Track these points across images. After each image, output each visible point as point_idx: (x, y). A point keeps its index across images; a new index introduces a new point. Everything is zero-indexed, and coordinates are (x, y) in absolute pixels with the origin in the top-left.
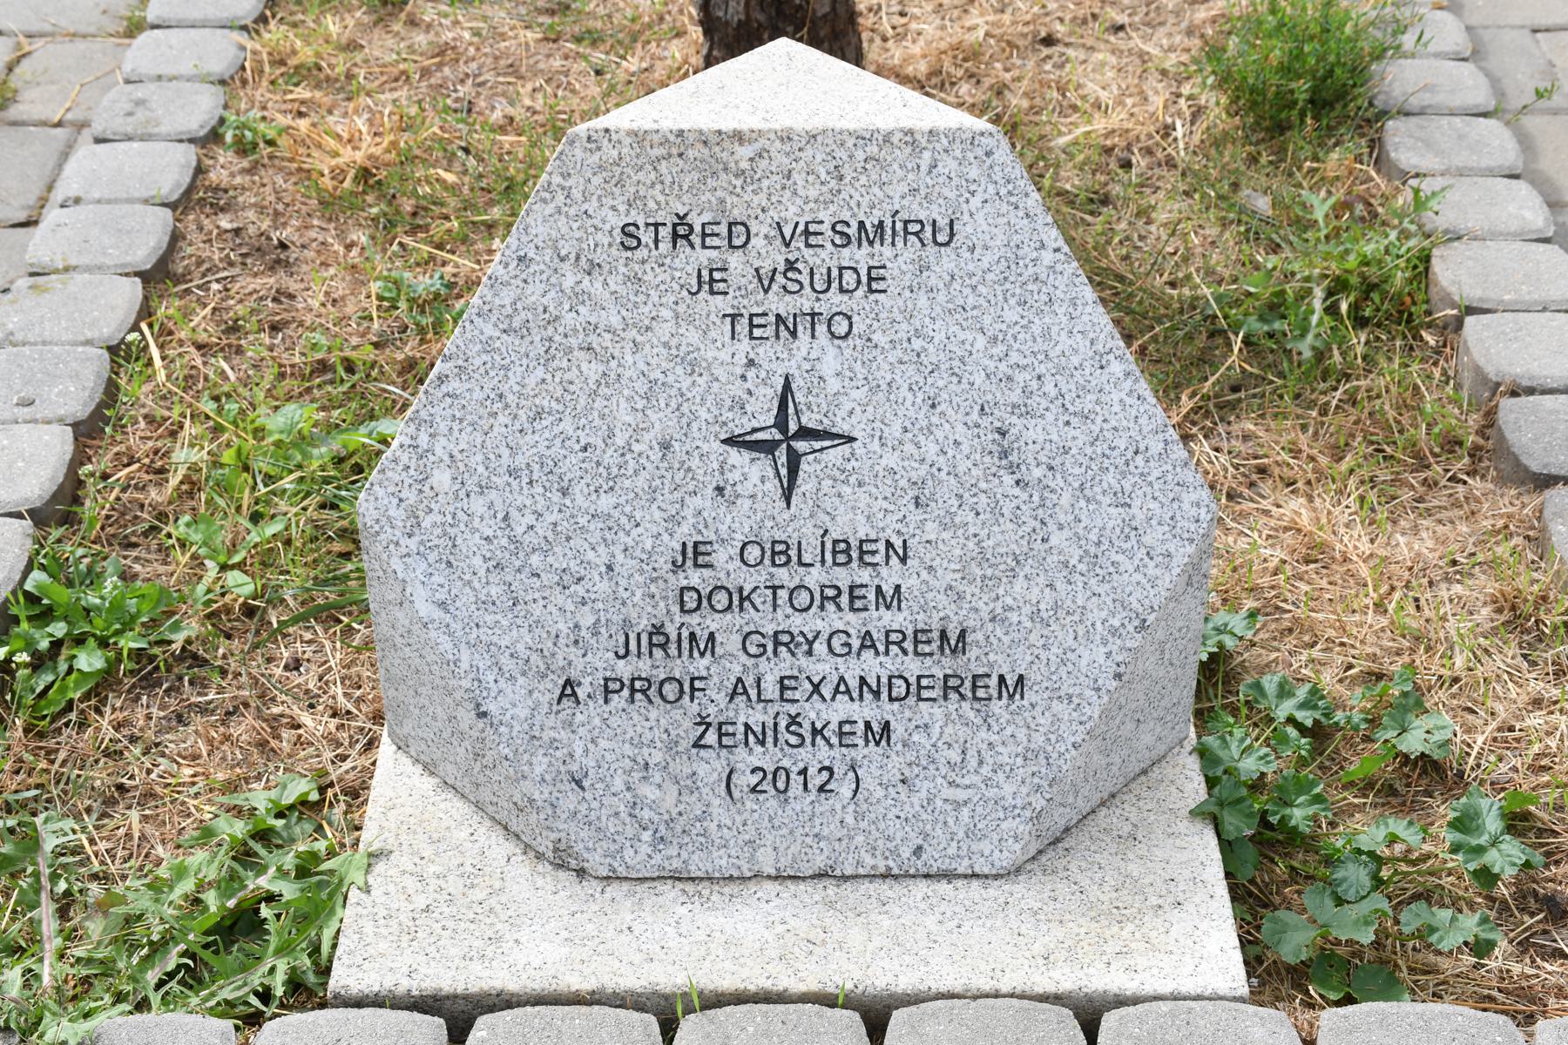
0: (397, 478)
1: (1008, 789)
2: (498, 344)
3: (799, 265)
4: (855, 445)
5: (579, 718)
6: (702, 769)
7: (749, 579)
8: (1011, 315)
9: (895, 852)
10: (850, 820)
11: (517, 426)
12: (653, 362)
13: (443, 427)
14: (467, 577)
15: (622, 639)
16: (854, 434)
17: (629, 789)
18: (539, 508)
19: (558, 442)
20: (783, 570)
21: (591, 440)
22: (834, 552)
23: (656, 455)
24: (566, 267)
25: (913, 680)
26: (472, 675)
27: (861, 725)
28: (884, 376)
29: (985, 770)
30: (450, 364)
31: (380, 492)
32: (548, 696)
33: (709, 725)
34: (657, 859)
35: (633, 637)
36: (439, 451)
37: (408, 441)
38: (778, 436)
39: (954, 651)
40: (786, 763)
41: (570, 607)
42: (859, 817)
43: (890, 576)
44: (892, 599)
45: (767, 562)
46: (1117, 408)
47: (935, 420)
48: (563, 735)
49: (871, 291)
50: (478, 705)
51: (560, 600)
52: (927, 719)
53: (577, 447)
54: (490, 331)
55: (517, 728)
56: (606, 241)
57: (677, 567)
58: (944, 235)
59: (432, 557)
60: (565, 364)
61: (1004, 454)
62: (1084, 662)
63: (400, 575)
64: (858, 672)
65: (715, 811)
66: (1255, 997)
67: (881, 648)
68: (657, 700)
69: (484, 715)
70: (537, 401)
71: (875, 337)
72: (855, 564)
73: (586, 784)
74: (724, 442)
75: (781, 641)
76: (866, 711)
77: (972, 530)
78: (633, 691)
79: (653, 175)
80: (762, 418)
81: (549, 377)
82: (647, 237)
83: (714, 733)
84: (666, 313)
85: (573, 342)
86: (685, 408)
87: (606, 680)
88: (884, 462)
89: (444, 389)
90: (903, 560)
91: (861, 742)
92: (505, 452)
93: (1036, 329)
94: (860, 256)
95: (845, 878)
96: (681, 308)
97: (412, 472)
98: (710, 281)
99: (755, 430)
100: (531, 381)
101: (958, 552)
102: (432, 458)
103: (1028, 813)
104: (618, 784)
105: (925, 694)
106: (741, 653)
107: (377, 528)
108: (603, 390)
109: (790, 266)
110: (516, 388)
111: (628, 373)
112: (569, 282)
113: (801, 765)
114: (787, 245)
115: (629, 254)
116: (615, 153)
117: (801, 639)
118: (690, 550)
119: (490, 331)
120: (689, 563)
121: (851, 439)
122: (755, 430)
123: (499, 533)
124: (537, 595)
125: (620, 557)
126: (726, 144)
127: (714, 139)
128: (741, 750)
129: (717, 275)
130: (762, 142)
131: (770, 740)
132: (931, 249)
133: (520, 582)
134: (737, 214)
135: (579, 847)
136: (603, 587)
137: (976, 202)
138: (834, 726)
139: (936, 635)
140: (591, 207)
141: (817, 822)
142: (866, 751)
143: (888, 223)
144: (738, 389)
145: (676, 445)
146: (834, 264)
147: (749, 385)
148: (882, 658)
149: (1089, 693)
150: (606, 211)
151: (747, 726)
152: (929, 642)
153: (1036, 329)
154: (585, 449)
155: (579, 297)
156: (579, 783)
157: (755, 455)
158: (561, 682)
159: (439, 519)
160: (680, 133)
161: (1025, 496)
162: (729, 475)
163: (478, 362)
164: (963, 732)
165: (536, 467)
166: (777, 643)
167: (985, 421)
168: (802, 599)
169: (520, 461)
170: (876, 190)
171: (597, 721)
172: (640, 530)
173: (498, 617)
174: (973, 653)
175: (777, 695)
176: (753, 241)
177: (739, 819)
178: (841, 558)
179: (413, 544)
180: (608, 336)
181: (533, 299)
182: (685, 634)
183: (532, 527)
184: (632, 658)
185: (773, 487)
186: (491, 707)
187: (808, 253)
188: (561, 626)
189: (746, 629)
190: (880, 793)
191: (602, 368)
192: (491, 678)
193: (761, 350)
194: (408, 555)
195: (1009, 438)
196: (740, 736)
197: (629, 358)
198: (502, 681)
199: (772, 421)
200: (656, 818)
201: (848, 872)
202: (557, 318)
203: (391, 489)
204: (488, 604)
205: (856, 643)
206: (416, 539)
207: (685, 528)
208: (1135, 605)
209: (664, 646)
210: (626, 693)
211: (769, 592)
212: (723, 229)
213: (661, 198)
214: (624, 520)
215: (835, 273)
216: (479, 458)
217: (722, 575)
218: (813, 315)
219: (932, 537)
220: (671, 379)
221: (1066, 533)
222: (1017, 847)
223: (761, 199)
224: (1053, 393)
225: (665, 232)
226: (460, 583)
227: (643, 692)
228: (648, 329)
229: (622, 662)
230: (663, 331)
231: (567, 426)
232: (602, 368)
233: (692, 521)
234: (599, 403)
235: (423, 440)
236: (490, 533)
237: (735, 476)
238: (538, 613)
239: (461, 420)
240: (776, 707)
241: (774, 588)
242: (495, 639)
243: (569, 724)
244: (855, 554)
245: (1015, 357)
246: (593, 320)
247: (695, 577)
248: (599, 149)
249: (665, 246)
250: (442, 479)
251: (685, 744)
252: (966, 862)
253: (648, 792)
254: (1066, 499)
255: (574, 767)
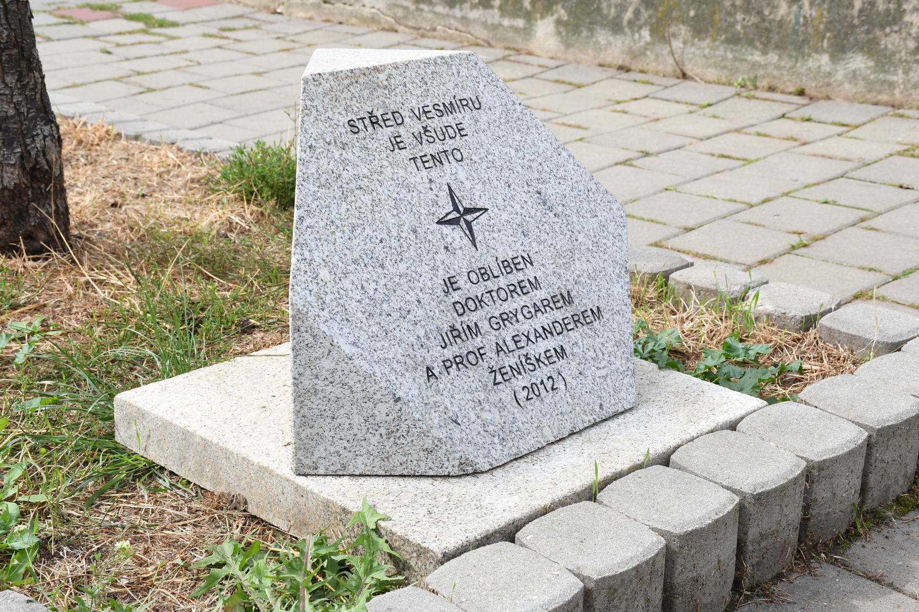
0: (304, 279)
1: (618, 363)
2: (319, 195)
3: (429, 128)
4: (489, 211)
5: (441, 386)
6: (503, 395)
7: (478, 290)
8: (518, 137)
9: (593, 410)
10: (570, 401)
11: (347, 237)
12: (391, 189)
13: (313, 245)
14: (359, 325)
15: (440, 338)
16: (487, 207)
17: (478, 417)
18: (375, 278)
19: (368, 240)
20: (489, 282)
21: (382, 236)
22: (505, 267)
23: (413, 237)
24: (332, 147)
25: (561, 322)
26: (384, 379)
27: (553, 351)
28: (485, 176)
29: (606, 357)
30: (302, 210)
31: (298, 289)
32: (423, 379)
33: (495, 371)
34: (506, 451)
35: (444, 335)
36: (317, 259)
37: (300, 257)
38: (458, 215)
39: (569, 303)
40: (534, 380)
41: (411, 328)
42: (573, 397)
43: (531, 272)
44: (535, 284)
45: (481, 280)
46: (573, 172)
47: (512, 192)
48: (438, 398)
49: (462, 136)
50: (394, 395)
51: (405, 325)
52: (575, 340)
53: (378, 241)
54: (313, 188)
55: (417, 401)
56: (344, 131)
57: (447, 293)
58: (475, 104)
59: (338, 318)
60: (353, 199)
61: (545, 203)
62: (615, 293)
63: (328, 333)
64: (540, 325)
65: (517, 415)
66: (770, 404)
67: (543, 310)
68: (469, 365)
69: (399, 399)
70: (350, 221)
71: (473, 157)
72: (515, 271)
73: (459, 421)
74: (438, 223)
75: (505, 318)
76: (551, 343)
77: (550, 242)
78: (457, 364)
79: (349, 94)
80: (447, 207)
81: (349, 207)
82: (361, 126)
83: (500, 376)
84: (385, 163)
85: (352, 186)
86: (414, 210)
87: (443, 362)
88: (503, 217)
89: (305, 224)
90: (531, 263)
91: (556, 359)
92: (348, 252)
93: (529, 142)
94: (448, 119)
95: (580, 432)
96: (391, 159)
97: (309, 274)
98: (397, 143)
99: (447, 214)
100: (343, 211)
101: (549, 254)
102: (315, 264)
103: (630, 373)
104: (473, 417)
105: (569, 327)
106: (491, 330)
107: (305, 310)
108: (376, 209)
109: (425, 129)
110: (338, 216)
111: (383, 197)
112: (337, 155)
113: (540, 379)
114: (420, 119)
115: (356, 136)
116: (328, 85)
117: (511, 315)
118: (448, 283)
119: (313, 188)
120: (450, 289)
121: (486, 210)
122: (447, 214)
123: (363, 297)
124: (394, 326)
125: (421, 294)
126: (373, 73)
127: (367, 72)
128: (513, 380)
129: (398, 140)
130: (387, 72)
131: (522, 371)
132: (475, 111)
133: (384, 320)
134: (393, 107)
135: (471, 457)
136: (420, 312)
137: (481, 86)
138: (543, 355)
139: (559, 297)
140: (330, 114)
141: (558, 406)
142: (560, 363)
143: (454, 102)
144: (431, 195)
145: (418, 229)
146: (442, 125)
147: (435, 192)
148: (545, 315)
149: (624, 307)
150: (337, 116)
151: (510, 366)
152: (558, 301)
153: (529, 142)
154: (381, 241)
155: (345, 162)
156: (456, 422)
157: (453, 227)
158: (425, 369)
159: (332, 296)
160: (352, 71)
161: (560, 221)
162: (447, 240)
163: (314, 206)
164: (590, 341)
165: (364, 256)
166: (503, 320)
167: (531, 189)
168: (503, 295)
169: (356, 255)
170: (442, 87)
171: (449, 385)
172: (423, 278)
173: (382, 343)
174: (576, 301)
175: (514, 347)
176: (405, 120)
177: (528, 416)
178: (509, 270)
179: (325, 313)
180: (366, 180)
181: (325, 167)
182: (465, 327)
183: (376, 290)
184: (449, 347)
185: (466, 241)
186: (400, 394)
187: (429, 121)
188: (412, 339)
189: (489, 317)
190: (575, 383)
191: (370, 197)
192: (393, 378)
193: (432, 173)
194: (327, 321)
195: (543, 195)
196: (510, 373)
197: (379, 189)
198: (399, 377)
199: (452, 209)
200: (496, 429)
201: (581, 428)
202: (340, 175)
203: (303, 286)
204: (374, 337)
205: (533, 310)
206: (327, 310)
207: (441, 272)
208: (620, 261)
209: (459, 336)
210: (454, 366)
211: (488, 295)
212: (390, 116)
213: (358, 105)
214: (414, 275)
215: (444, 130)
216: (337, 258)
217: (466, 292)
218: (445, 152)
219: (537, 250)
220: (402, 196)
221: (582, 235)
222: (634, 390)
223: (399, 99)
224: (548, 170)
225: (367, 122)
226: (357, 329)
227: (461, 363)
228: (381, 172)
229: (446, 350)
230: (388, 171)
231: (368, 231)
232: (370, 197)
233: (442, 267)
234: (377, 216)
235: (307, 254)
236: (358, 298)
237: (449, 240)
238: (398, 335)
239: (320, 239)
240: (517, 353)
241: (490, 292)
242: (386, 355)
243: (438, 391)
244: (512, 266)
245: (528, 157)
246: (356, 173)
247: (456, 296)
248: (320, 84)
249: (370, 129)
250: (324, 274)
251: (490, 384)
252: (620, 405)
253: (486, 416)
254: (575, 219)
255: (451, 414)
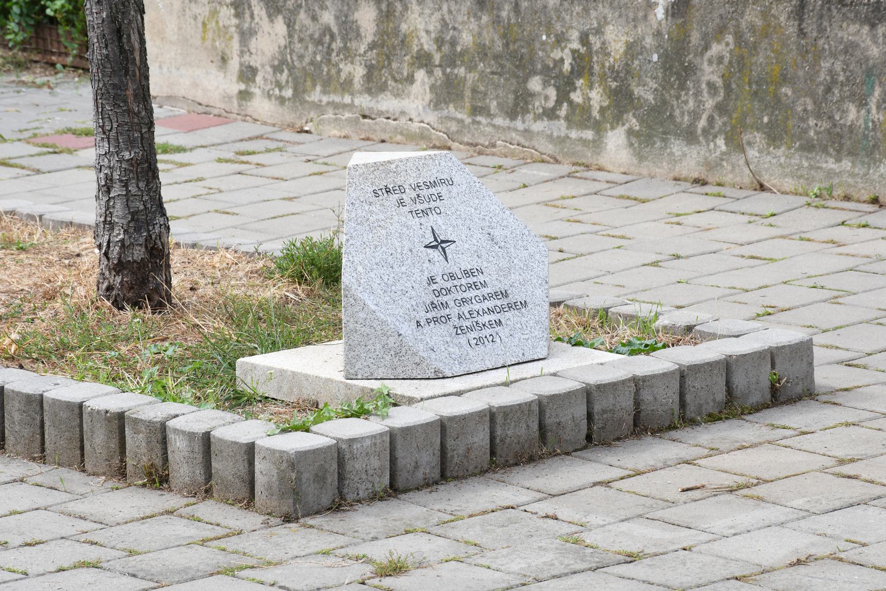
6: (461, 341)
7: (449, 285)
8: (477, 202)
24: (364, 204)
42: (505, 347)
43: (481, 278)
44: (484, 285)
48: (423, 337)
54: (354, 225)
58: (450, 182)
61: (493, 240)
75: (464, 301)
76: (493, 317)
82: (380, 193)
83: (460, 330)
85: (375, 225)
94: (433, 190)
98: (401, 203)
100: (370, 237)
104: (443, 349)
109: (418, 196)
112: (367, 208)
119: (354, 225)
134: (399, 183)
136: (413, 293)
137: (454, 172)
140: (363, 186)
144: (421, 232)
153: (484, 204)
155: (371, 212)
164: (519, 319)
168: (463, 288)
169: (377, 261)
174: (511, 296)
207: (426, 273)
223: (402, 179)
225: (384, 191)
230: (396, 218)
231: (384, 249)
235: (351, 258)
243: (423, 334)
245: (483, 213)
247: (435, 287)
249: (385, 195)
250: (360, 268)
251: (454, 334)
254: (513, 250)
